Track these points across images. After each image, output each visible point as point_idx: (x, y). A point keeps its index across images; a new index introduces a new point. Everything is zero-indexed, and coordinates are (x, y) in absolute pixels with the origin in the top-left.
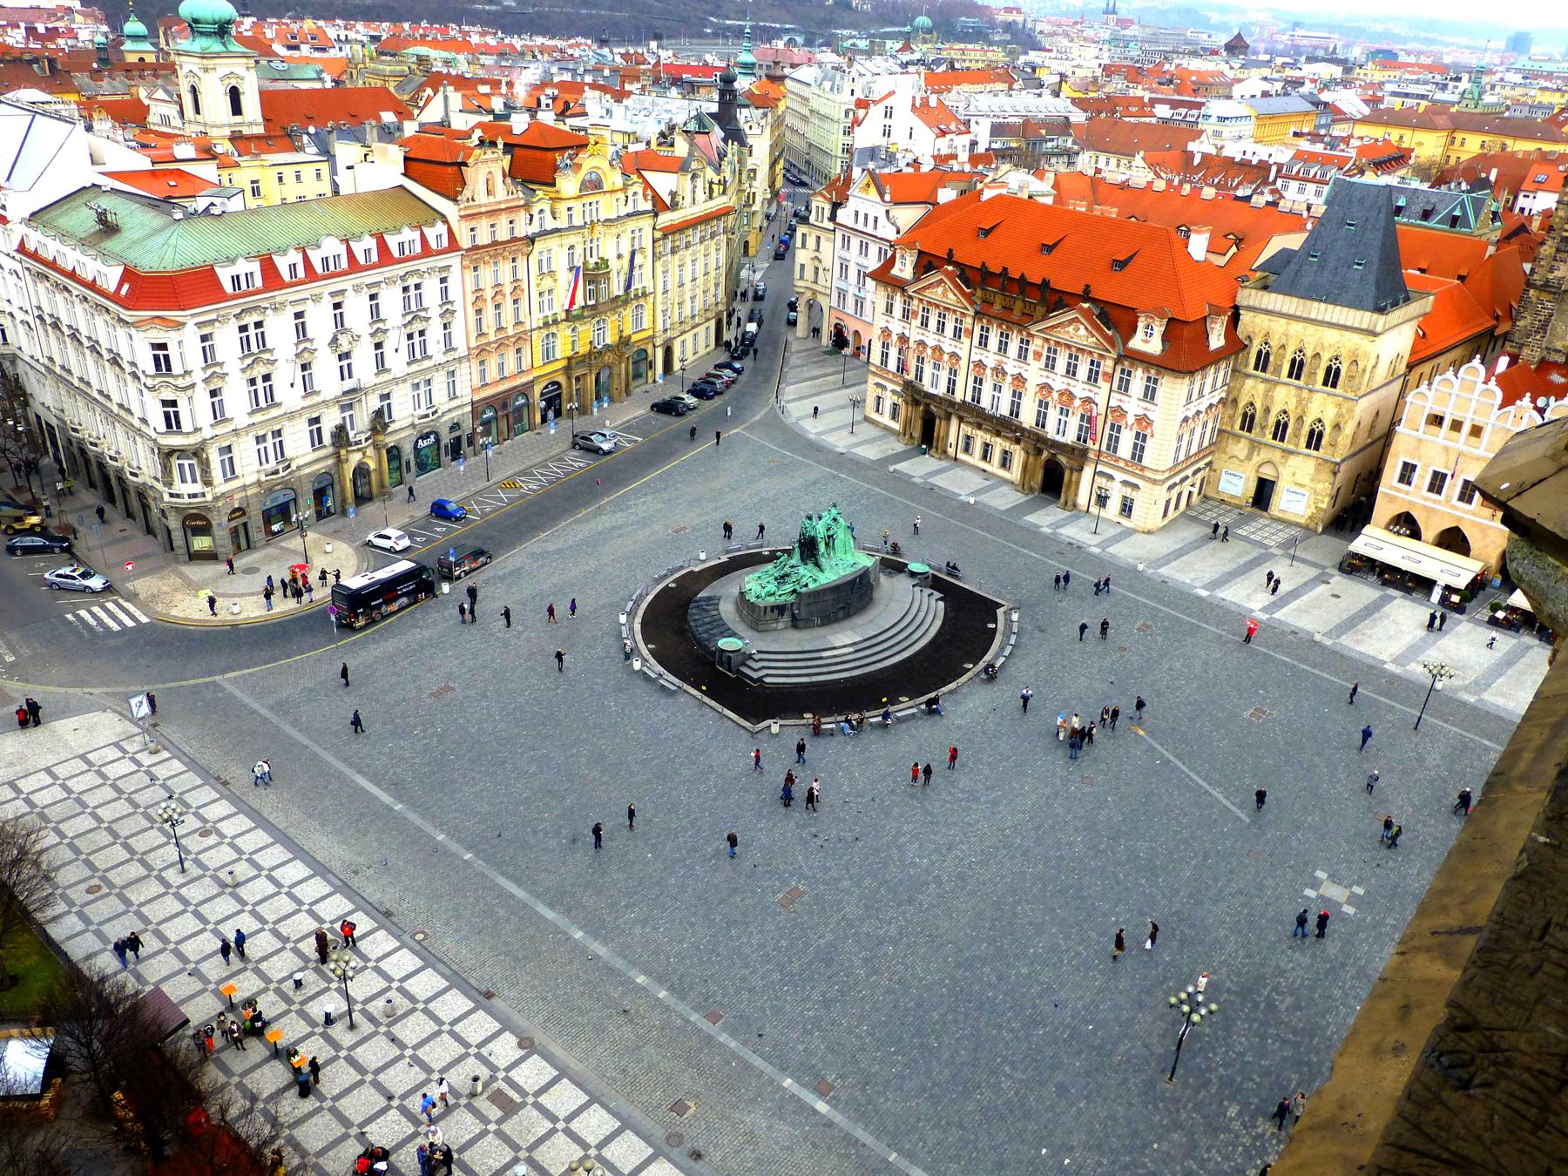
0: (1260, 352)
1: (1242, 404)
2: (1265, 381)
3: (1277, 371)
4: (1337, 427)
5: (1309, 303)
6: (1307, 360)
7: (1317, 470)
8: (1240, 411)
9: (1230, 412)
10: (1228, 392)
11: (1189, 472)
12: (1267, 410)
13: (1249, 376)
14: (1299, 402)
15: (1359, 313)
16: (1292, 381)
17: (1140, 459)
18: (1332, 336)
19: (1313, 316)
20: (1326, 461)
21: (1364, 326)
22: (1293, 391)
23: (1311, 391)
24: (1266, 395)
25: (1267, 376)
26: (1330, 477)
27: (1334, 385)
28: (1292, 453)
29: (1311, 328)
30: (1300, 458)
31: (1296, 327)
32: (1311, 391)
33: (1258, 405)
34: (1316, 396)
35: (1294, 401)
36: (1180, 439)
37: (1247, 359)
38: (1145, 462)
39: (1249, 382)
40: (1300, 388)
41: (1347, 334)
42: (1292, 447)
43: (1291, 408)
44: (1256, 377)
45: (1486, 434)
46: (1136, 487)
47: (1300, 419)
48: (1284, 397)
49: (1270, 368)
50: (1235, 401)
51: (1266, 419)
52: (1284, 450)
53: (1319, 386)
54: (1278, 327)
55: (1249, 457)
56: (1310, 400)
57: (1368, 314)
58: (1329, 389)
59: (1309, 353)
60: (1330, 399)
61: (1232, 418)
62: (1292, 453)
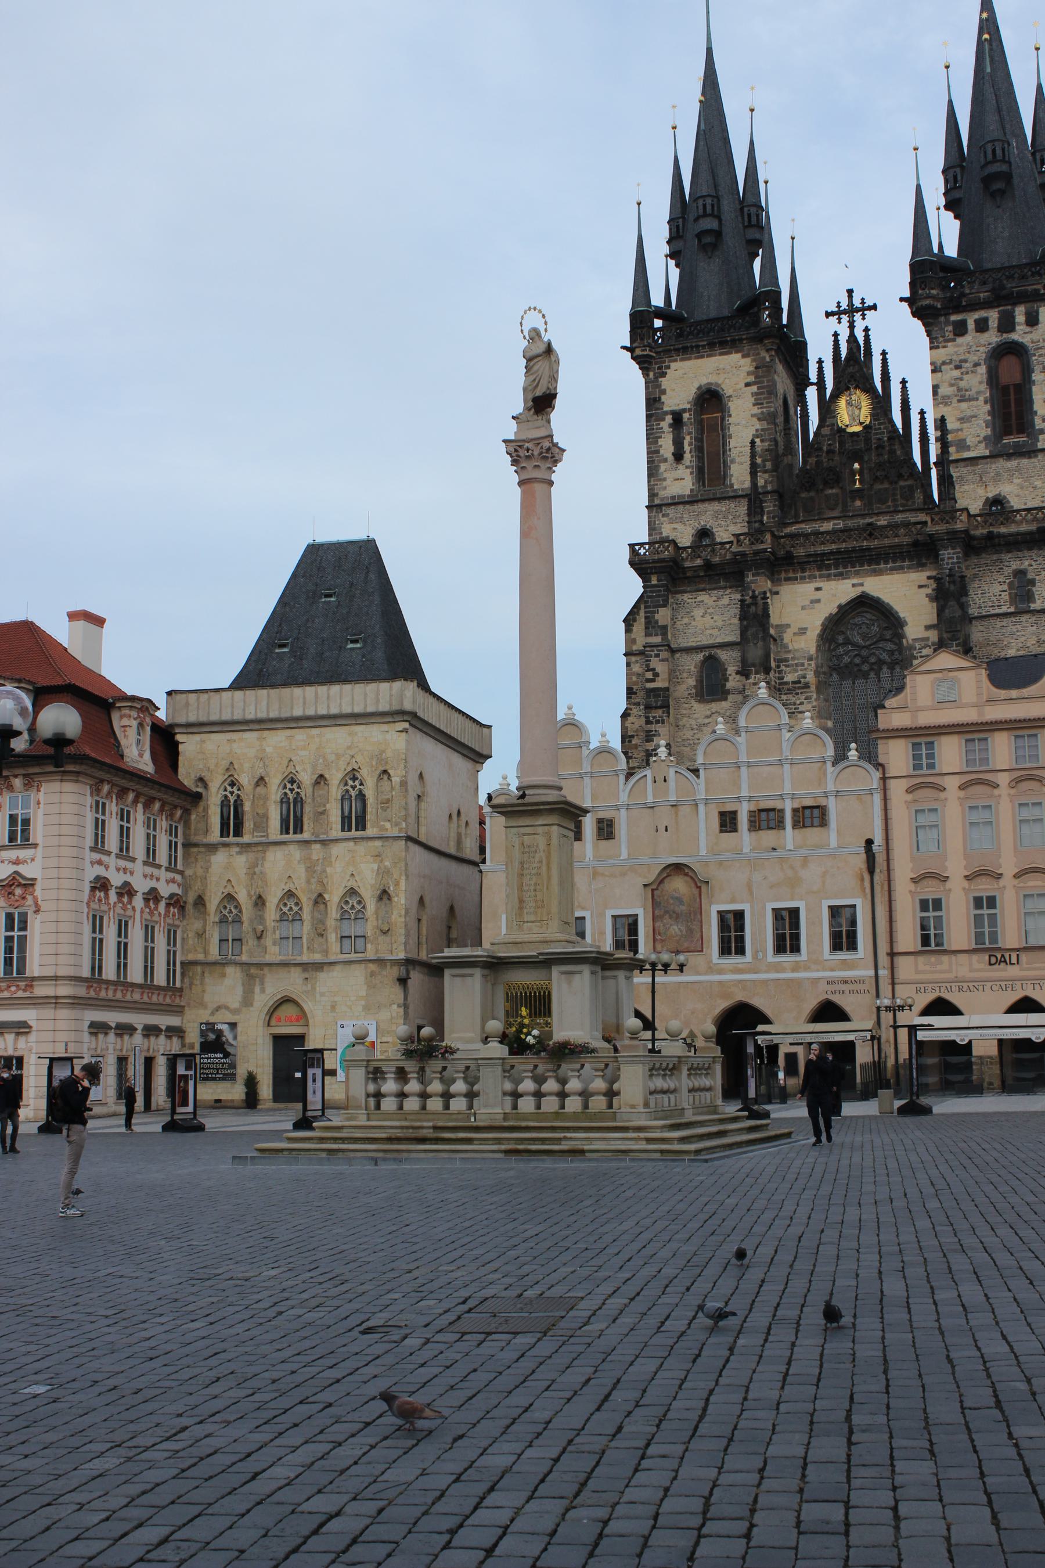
0: (225, 803)
1: (213, 903)
2: (246, 847)
3: (262, 823)
4: (384, 895)
5: (286, 692)
6: (307, 791)
7: (371, 986)
8: (213, 917)
9: (197, 925)
10: (186, 887)
11: (139, 1020)
12: (260, 902)
13: (213, 848)
14: (310, 870)
15: (371, 687)
16: (291, 836)
17: (21, 970)
18: (337, 737)
19: (298, 712)
20: (380, 962)
21: (384, 707)
22: (296, 852)
23: (324, 843)
24: (252, 874)
25: (246, 838)
26: (397, 993)
27: (361, 824)
28: (319, 967)
29: (300, 736)
30: (337, 972)
31: (276, 740)
32: (324, 843)
33: (242, 897)
34: (336, 850)
35: (301, 872)
36: (97, 924)
37: (205, 817)
38: (34, 968)
39: (219, 858)
40: (307, 842)
41: (360, 730)
42: (317, 957)
43: (300, 884)
44: (226, 845)
45: (622, 830)
46: (21, 1028)
47: (319, 900)
48: (283, 867)
49: (248, 825)
50: (200, 902)
51: (261, 919)
52: (305, 966)
53: (336, 832)
54: (244, 749)
55: (247, 1001)
56: (327, 861)
57: (384, 686)
58: (354, 833)
59: (306, 778)
60: (361, 848)
61: (200, 935)
62: (319, 967)
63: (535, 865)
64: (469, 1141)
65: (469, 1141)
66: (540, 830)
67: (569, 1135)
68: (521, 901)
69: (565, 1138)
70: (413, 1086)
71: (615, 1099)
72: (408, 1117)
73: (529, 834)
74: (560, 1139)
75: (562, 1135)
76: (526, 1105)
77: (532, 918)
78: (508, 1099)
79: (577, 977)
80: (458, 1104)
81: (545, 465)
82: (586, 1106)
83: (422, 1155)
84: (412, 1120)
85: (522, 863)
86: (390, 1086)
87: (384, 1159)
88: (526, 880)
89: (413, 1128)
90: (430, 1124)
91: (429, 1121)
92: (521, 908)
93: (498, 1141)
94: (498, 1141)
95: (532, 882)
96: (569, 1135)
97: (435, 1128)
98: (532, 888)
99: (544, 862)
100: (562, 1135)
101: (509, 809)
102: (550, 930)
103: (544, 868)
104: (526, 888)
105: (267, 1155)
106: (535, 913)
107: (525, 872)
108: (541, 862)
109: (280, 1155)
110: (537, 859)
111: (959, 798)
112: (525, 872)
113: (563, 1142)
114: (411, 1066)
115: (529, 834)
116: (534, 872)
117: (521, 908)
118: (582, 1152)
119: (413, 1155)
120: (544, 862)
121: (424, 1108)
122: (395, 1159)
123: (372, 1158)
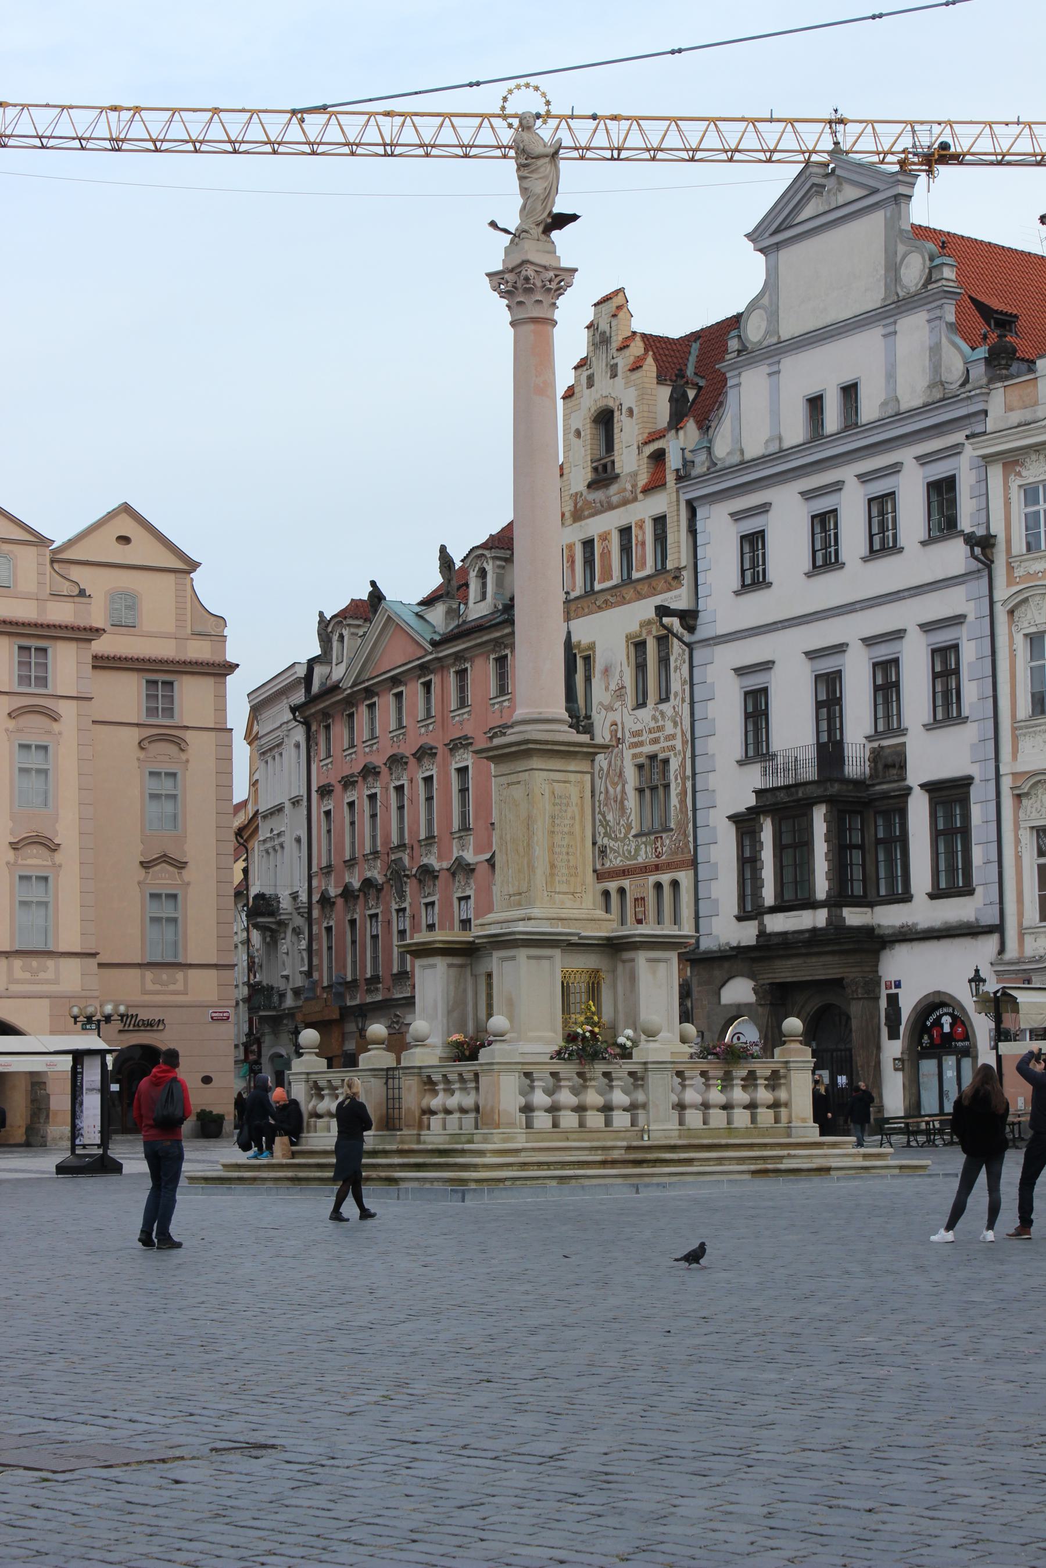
63: (567, 822)
64: (689, 1161)
65: (689, 1161)
66: (572, 777)
67: (792, 1152)
68: (553, 866)
69: (789, 1156)
70: (566, 1097)
71: (783, 1111)
72: (570, 1135)
73: (558, 781)
74: (783, 1157)
75: (785, 1152)
76: (694, 1119)
77: (564, 888)
78: (675, 1114)
79: (662, 966)
80: (621, 1120)
81: (547, 300)
82: (754, 1120)
83: (666, 1180)
84: (574, 1140)
85: (553, 817)
86: (540, 1098)
87: (647, 1185)
88: (557, 839)
89: (604, 1148)
90: (625, 1144)
91: (623, 1139)
92: (552, 875)
93: (741, 1160)
94: (741, 1160)
95: (565, 843)
96: (792, 1152)
97: (629, 1148)
98: (564, 850)
99: (577, 818)
100: (785, 1152)
101: (549, 747)
102: (584, 906)
103: (577, 827)
104: (557, 850)
105: (485, 1186)
106: (568, 882)
107: (557, 829)
108: (573, 818)
109: (501, 1185)
110: (569, 815)
111: (7, 730)
112: (557, 829)
113: (784, 1161)
114: (568, 1070)
115: (558, 781)
116: (566, 830)
117: (552, 875)
118: (828, 1170)
119: (655, 1180)
120: (577, 818)
121: (582, 1124)
122: (658, 1185)
123: (633, 1185)
